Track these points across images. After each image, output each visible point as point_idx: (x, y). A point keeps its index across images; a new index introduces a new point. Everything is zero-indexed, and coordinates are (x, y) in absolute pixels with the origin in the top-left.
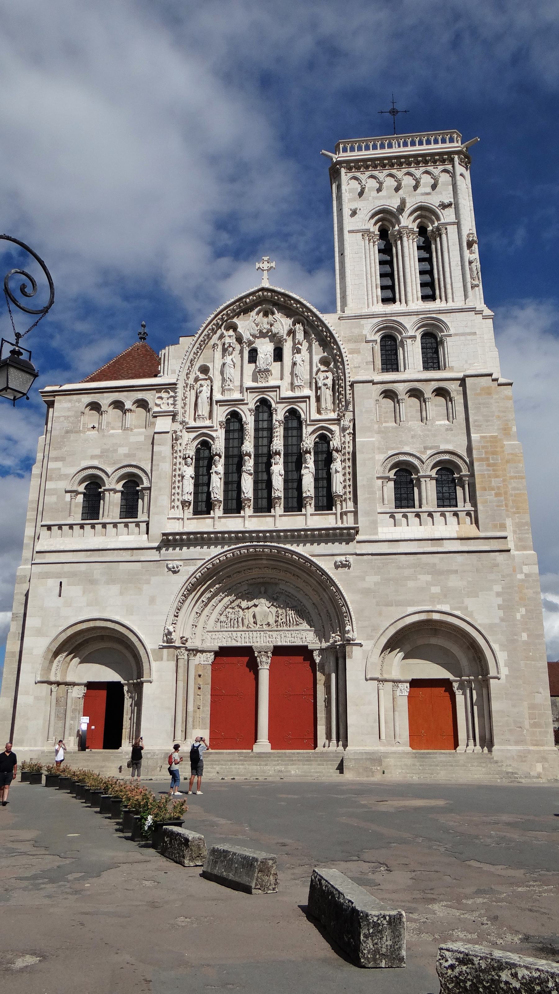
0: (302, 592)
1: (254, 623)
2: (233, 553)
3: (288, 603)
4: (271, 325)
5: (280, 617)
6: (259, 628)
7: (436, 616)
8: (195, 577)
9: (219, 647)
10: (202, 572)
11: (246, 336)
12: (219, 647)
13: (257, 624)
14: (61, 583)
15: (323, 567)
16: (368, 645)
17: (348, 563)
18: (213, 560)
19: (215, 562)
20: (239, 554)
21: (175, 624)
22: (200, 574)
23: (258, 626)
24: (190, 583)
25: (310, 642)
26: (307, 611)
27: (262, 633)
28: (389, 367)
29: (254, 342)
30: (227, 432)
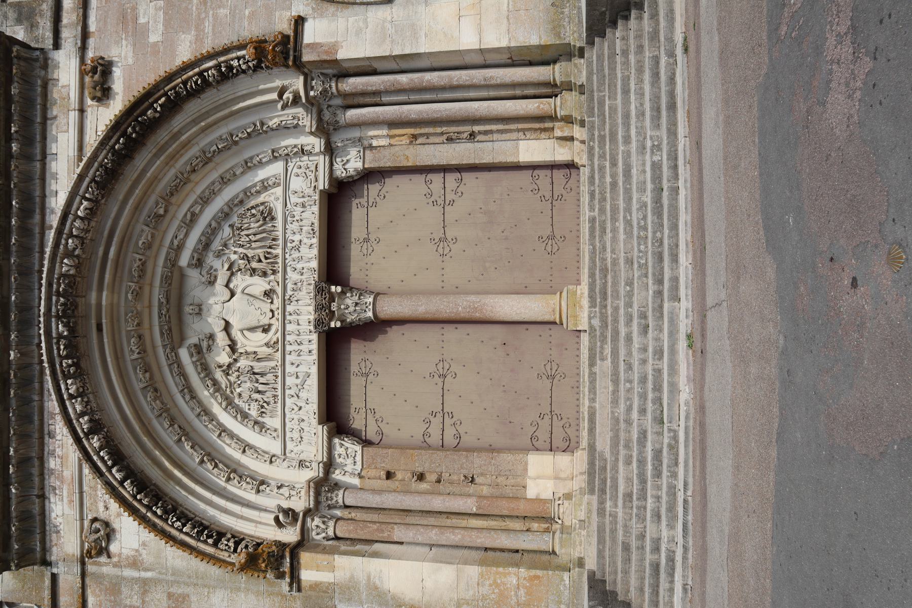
0: (197, 209)
2: (66, 377)
5: (254, 265)
6: (278, 320)
9: (319, 424)
10: (110, 463)
12: (319, 424)
13: (270, 325)
15: (102, 129)
18: (79, 431)
19: (85, 427)
20: (70, 361)
23: (273, 321)
24: (134, 497)
25: (313, 185)
26: (241, 195)
27: (289, 308)
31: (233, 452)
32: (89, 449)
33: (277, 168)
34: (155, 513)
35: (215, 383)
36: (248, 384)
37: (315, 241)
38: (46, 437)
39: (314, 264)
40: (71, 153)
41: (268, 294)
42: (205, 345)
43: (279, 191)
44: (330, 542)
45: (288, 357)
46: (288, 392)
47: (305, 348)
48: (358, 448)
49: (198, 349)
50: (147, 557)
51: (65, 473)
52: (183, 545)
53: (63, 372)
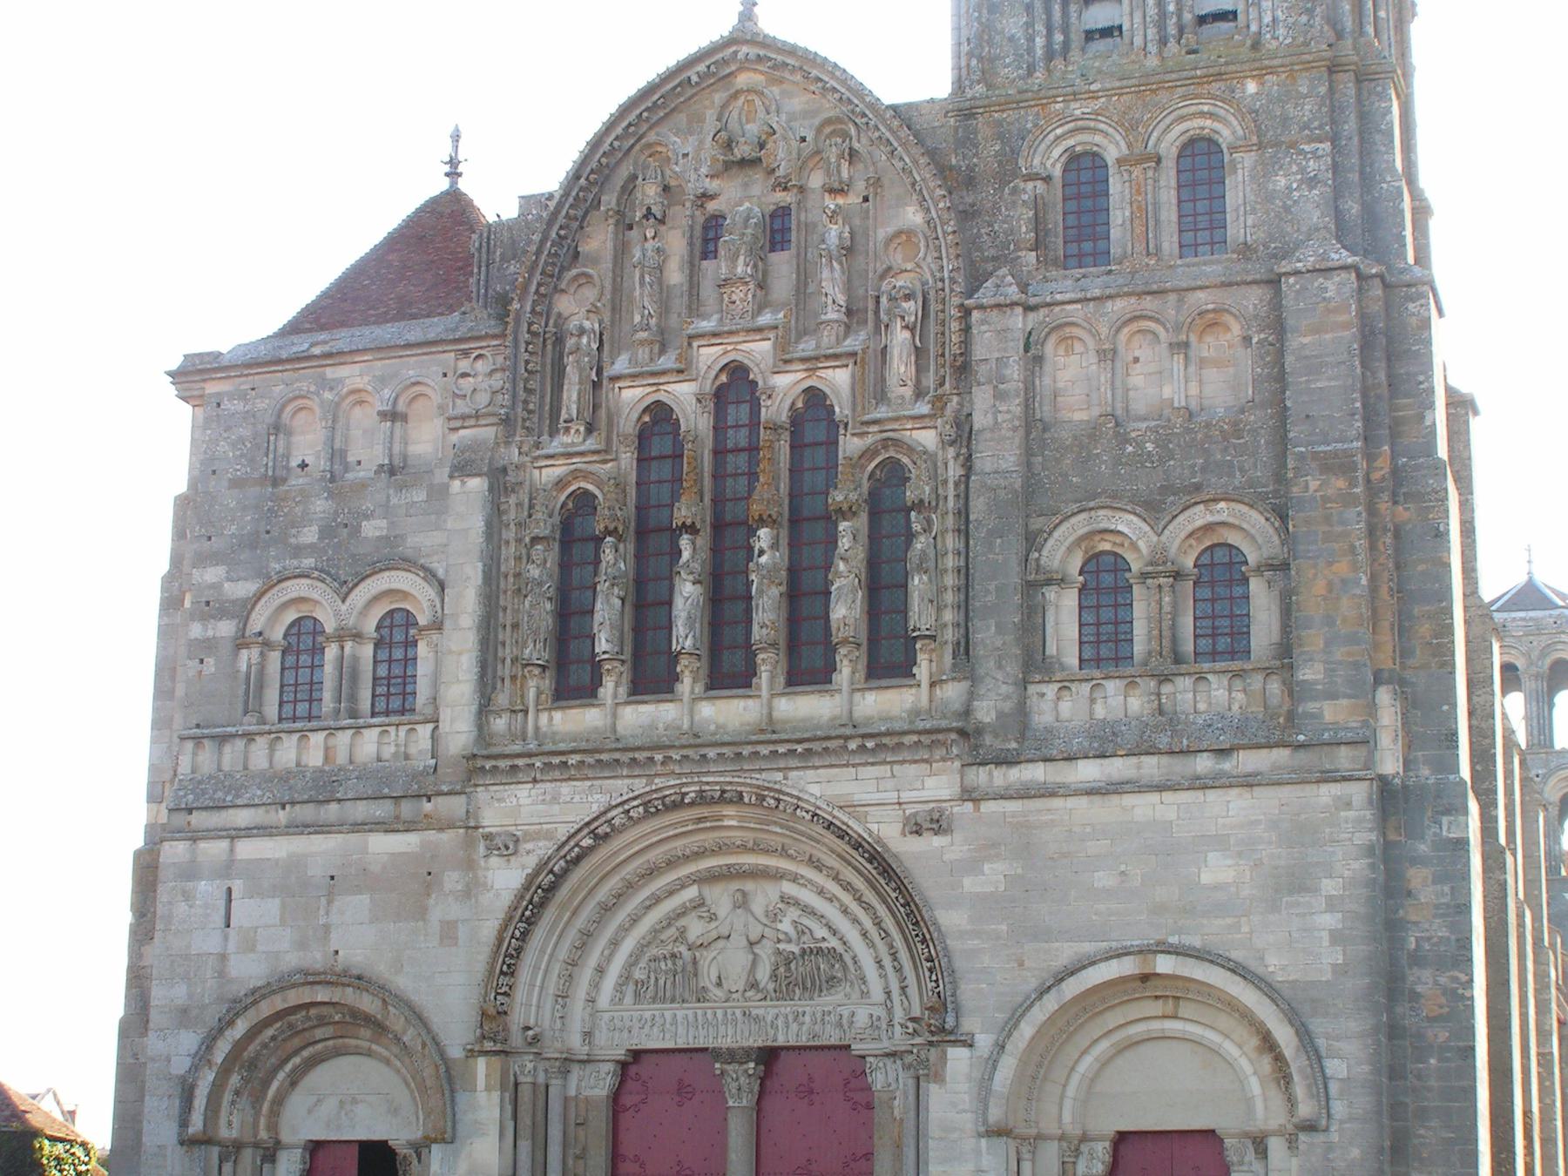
1: (719, 984)
3: (803, 932)
4: (762, 146)
5: (782, 970)
7: (1164, 965)
8: (551, 871)
10: (568, 858)
11: (696, 179)
14: (229, 890)
16: (984, 1041)
17: (935, 826)
18: (596, 824)
21: (505, 994)
22: (562, 863)
24: (539, 887)
28: (1087, 246)
29: (712, 197)
30: (641, 461)
31: (593, 960)
32: (579, 836)
33: (877, 993)
34: (526, 909)
35: (669, 925)
36: (663, 967)
37: (804, 1040)
38: (588, 783)
39: (781, 1041)
40: (856, 797)
41: (754, 985)
42: (702, 911)
43: (856, 995)
44: (512, 1078)
45: (690, 1013)
46: (657, 1013)
47: (702, 1033)
48: (604, 1093)
49: (699, 904)
50: (486, 898)
51: (557, 807)
52: (500, 940)
53: (650, 801)
